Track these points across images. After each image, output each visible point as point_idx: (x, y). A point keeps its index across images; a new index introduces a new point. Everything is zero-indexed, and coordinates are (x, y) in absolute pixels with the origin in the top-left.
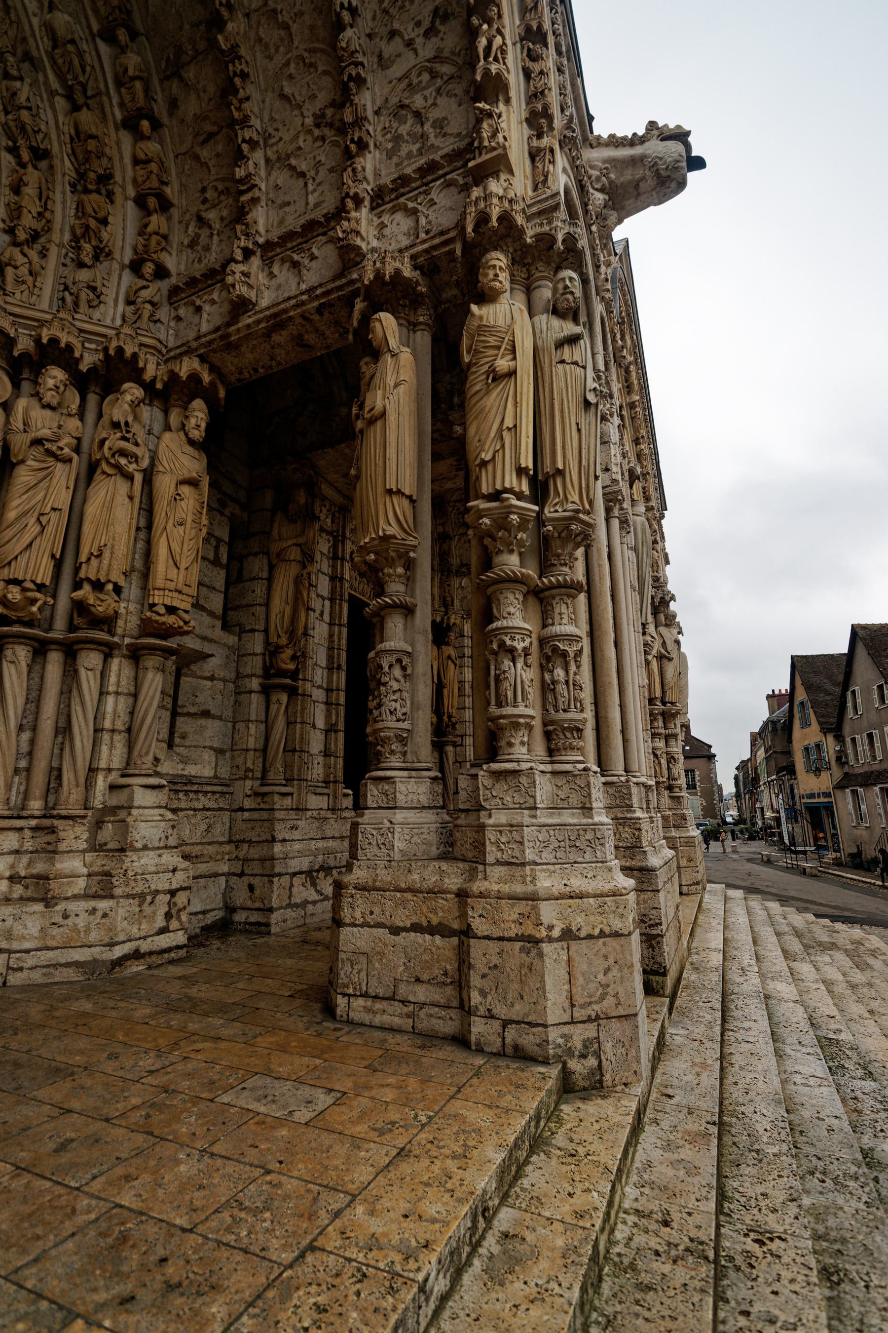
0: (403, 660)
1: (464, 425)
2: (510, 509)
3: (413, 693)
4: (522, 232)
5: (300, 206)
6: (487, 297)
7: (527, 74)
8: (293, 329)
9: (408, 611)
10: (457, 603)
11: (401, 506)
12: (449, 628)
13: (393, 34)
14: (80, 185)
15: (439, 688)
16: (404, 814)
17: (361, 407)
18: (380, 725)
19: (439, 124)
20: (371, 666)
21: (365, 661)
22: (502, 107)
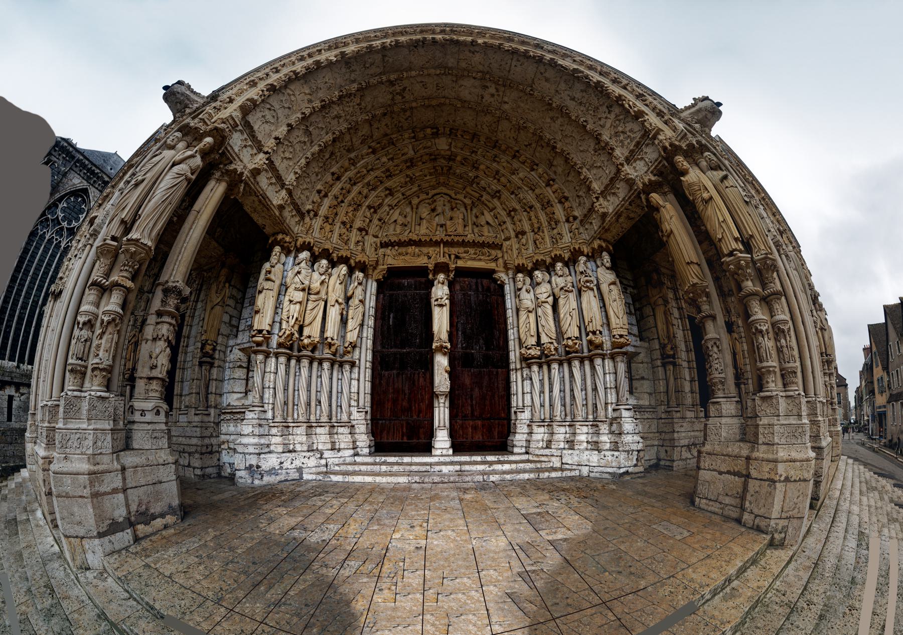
0: (717, 342)
1: (704, 225)
2: (739, 259)
3: (724, 358)
4: (680, 147)
5: (605, 175)
6: (684, 173)
7: (646, 105)
8: (624, 215)
9: (713, 318)
10: (733, 311)
11: (695, 268)
12: (732, 323)
13: (600, 119)
14: (544, 208)
15: (734, 355)
16: (725, 420)
17: (662, 231)
18: (712, 376)
19: (631, 131)
20: (704, 347)
21: (701, 346)
22: (647, 117)
